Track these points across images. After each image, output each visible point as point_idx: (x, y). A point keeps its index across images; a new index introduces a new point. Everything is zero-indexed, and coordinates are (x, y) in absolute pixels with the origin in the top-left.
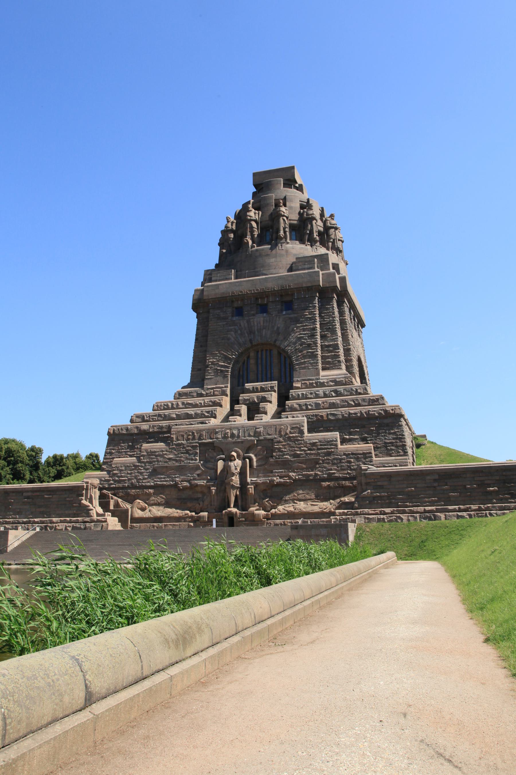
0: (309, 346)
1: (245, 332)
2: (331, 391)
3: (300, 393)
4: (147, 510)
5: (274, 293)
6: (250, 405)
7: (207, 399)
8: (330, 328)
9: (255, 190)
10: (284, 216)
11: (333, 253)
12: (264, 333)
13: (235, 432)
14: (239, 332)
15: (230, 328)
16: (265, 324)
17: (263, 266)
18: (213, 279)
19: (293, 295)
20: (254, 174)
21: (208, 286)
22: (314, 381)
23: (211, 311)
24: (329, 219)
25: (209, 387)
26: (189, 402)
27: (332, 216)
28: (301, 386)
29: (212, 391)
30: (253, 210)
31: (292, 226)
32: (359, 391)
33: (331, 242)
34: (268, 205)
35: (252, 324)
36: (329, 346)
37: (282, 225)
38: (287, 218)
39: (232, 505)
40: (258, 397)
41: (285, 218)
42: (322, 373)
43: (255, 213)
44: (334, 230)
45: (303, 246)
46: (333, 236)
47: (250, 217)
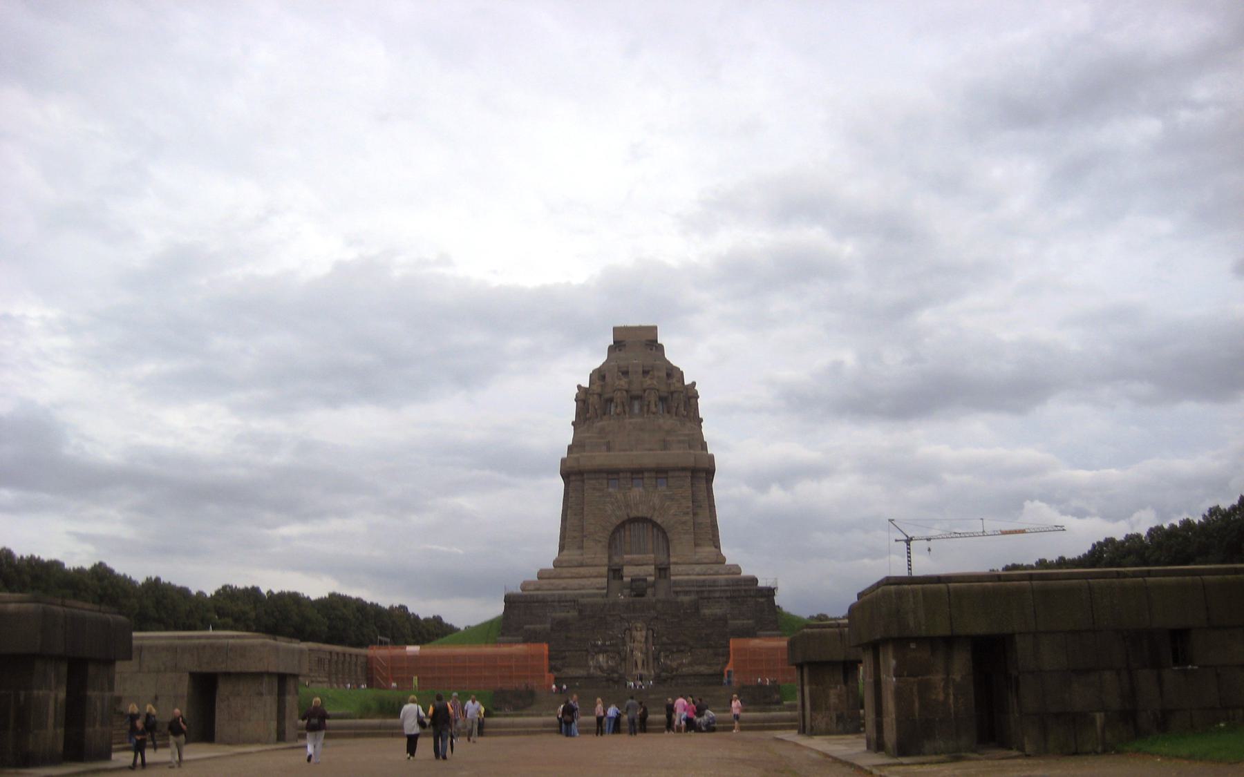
0: (684, 523)
5: (650, 470)
7: (592, 570)
20: (615, 329)
27: (694, 384)
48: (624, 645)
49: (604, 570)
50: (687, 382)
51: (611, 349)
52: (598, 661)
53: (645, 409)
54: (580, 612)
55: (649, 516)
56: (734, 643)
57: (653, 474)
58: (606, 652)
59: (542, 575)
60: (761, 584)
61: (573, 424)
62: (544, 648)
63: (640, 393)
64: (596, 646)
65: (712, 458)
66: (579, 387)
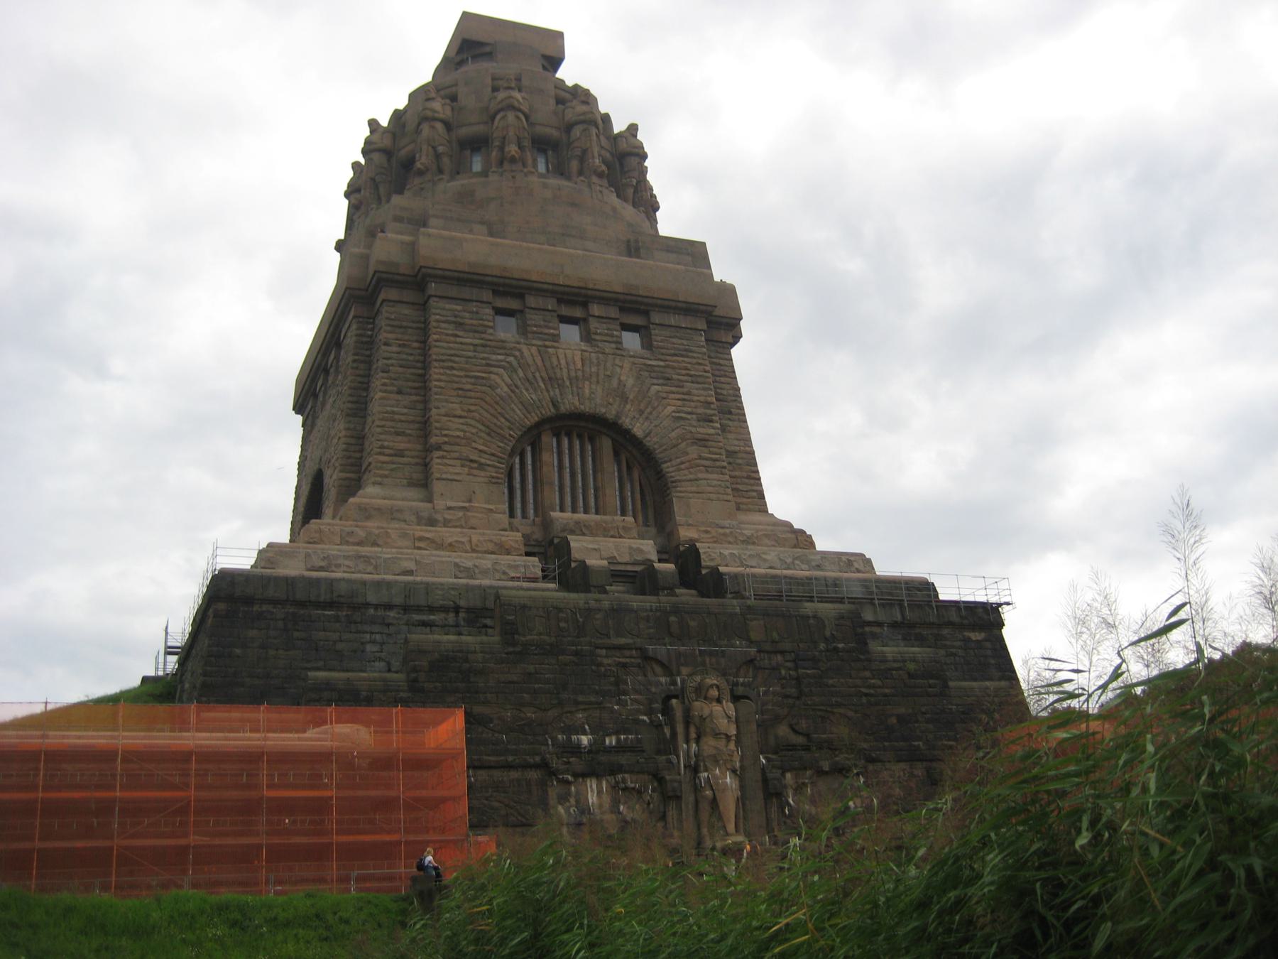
0: (702, 441)
1: (537, 375)
3: (726, 552)
5: (606, 298)
8: (730, 413)
12: (587, 391)
14: (521, 374)
15: (494, 357)
16: (587, 369)
18: (433, 221)
19: (646, 313)
20: (467, 18)
22: (728, 531)
23: (432, 302)
25: (450, 504)
29: (460, 514)
35: (555, 363)
39: (731, 827)
48: (669, 746)
52: (584, 809)
53: (574, 165)
54: (509, 632)
55: (611, 413)
57: (613, 312)
58: (614, 770)
62: (447, 730)
63: (555, 133)
64: (576, 750)
66: (373, 124)
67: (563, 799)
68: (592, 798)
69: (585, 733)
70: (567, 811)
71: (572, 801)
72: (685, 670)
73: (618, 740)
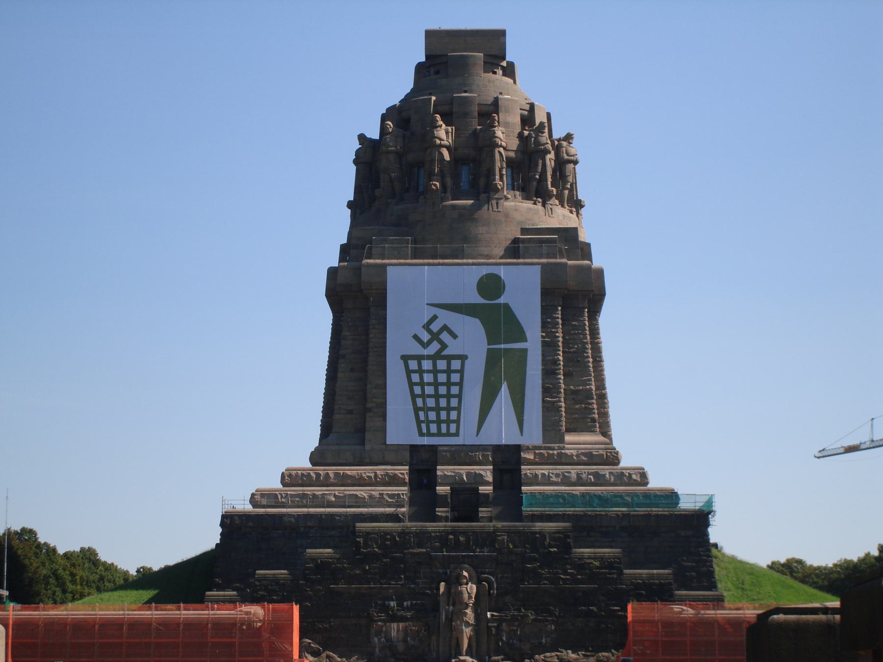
2: (589, 474)
3: (539, 472)
4: (324, 655)
6: (457, 486)
9: (423, 59)
10: (501, 146)
11: (571, 212)
13: (461, 539)
17: (466, 239)
18: (374, 251)
20: (429, 34)
21: (369, 266)
22: (555, 452)
24: (564, 144)
26: (349, 473)
27: (569, 138)
28: (535, 458)
30: (444, 126)
31: (510, 163)
32: (634, 477)
33: (567, 189)
34: (466, 115)
36: (575, 392)
37: (498, 164)
38: (505, 149)
40: (468, 474)
41: (501, 150)
42: (568, 438)
43: (447, 133)
44: (572, 165)
45: (528, 204)
46: (570, 179)
47: (441, 140)
48: (436, 609)
49: (403, 471)
50: (558, 134)
51: (419, 67)
56: (632, 611)
59: (290, 478)
60: (686, 504)
61: (350, 205)
65: (600, 273)
66: (362, 138)
67: (378, 633)
68: (394, 634)
69: (393, 600)
70: (379, 640)
71: (383, 635)
72: (452, 566)
73: (412, 604)
